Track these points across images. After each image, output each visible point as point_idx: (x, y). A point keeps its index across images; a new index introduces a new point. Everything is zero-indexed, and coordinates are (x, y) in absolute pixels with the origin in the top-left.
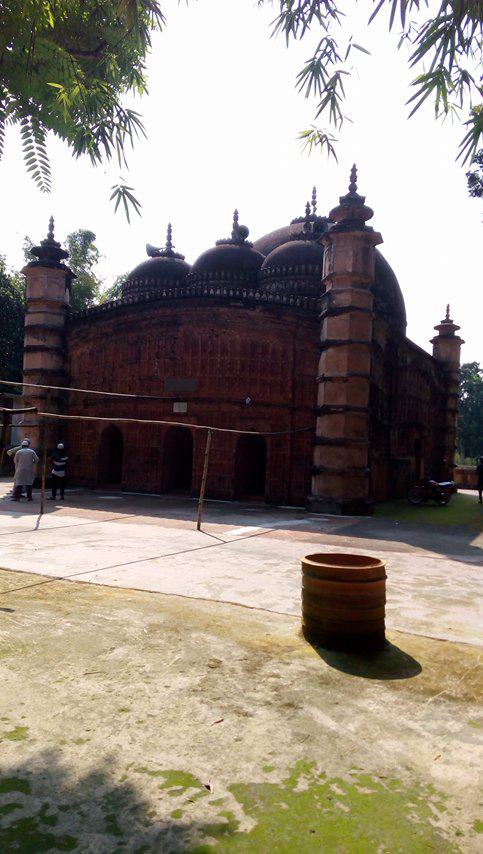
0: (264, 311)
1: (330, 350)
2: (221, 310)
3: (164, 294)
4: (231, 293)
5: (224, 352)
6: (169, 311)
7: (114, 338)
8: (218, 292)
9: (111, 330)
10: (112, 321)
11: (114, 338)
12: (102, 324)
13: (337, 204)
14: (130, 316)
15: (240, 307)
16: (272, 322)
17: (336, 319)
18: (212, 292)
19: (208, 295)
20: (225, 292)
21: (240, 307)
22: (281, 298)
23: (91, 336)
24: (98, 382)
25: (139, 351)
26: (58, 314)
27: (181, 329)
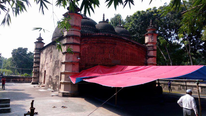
0: (136, 46)
1: (153, 58)
2: (127, 44)
3: (112, 35)
4: (128, 40)
5: (126, 54)
6: (113, 41)
7: (96, 45)
8: (125, 39)
9: (96, 42)
10: (96, 39)
11: (96, 45)
12: (93, 39)
13: (84, 12)
14: (102, 39)
15: (131, 44)
16: (138, 49)
17: (154, 51)
18: (124, 38)
19: (123, 39)
20: (127, 39)
21: (131, 44)
22: (139, 44)
23: (89, 43)
24: (90, 58)
25: (104, 50)
26: (78, 31)
27: (116, 46)
